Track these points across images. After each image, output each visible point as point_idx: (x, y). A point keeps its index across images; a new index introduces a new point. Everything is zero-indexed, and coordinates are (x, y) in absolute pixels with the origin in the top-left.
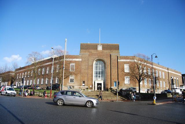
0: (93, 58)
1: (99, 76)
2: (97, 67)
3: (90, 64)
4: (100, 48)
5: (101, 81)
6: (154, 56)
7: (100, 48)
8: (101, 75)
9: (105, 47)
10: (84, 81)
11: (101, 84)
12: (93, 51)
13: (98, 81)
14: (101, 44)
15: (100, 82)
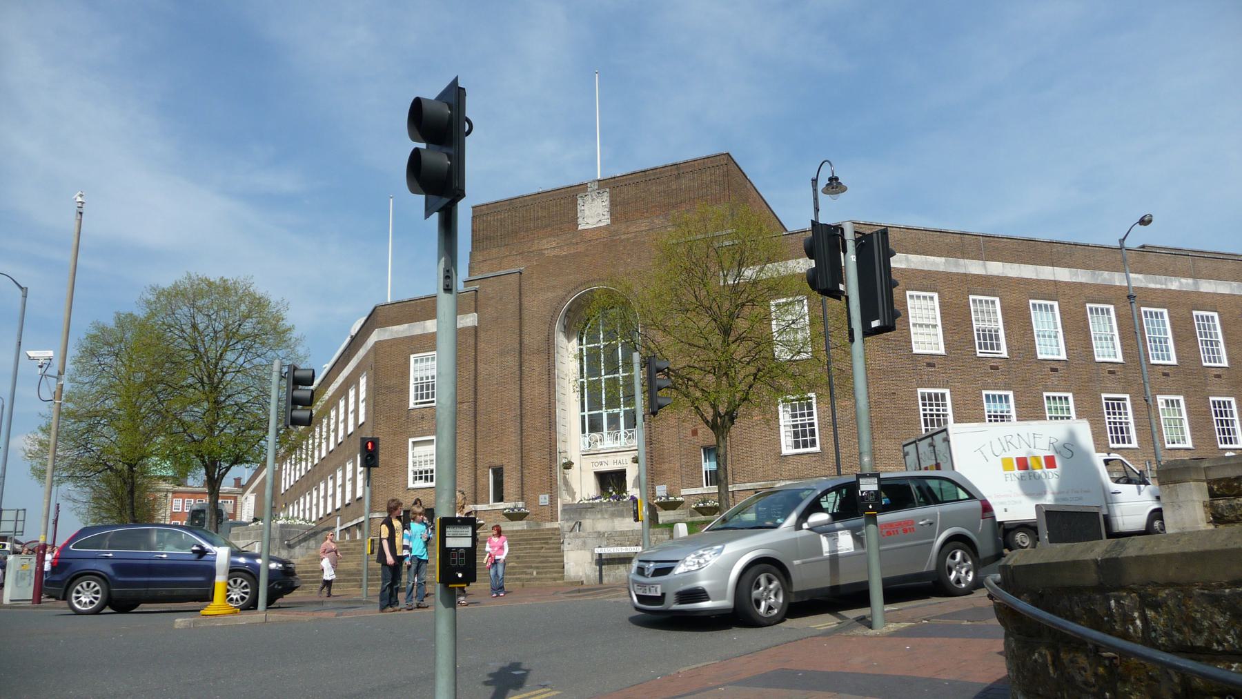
0: (550, 295)
1: (614, 420)
2: (593, 356)
3: (533, 339)
4: (594, 213)
5: (619, 457)
6: (823, 182)
7: (594, 213)
8: (621, 411)
9: (631, 192)
10: (496, 462)
11: (621, 474)
12: (549, 246)
13: (601, 458)
14: (604, 184)
15: (610, 465)
